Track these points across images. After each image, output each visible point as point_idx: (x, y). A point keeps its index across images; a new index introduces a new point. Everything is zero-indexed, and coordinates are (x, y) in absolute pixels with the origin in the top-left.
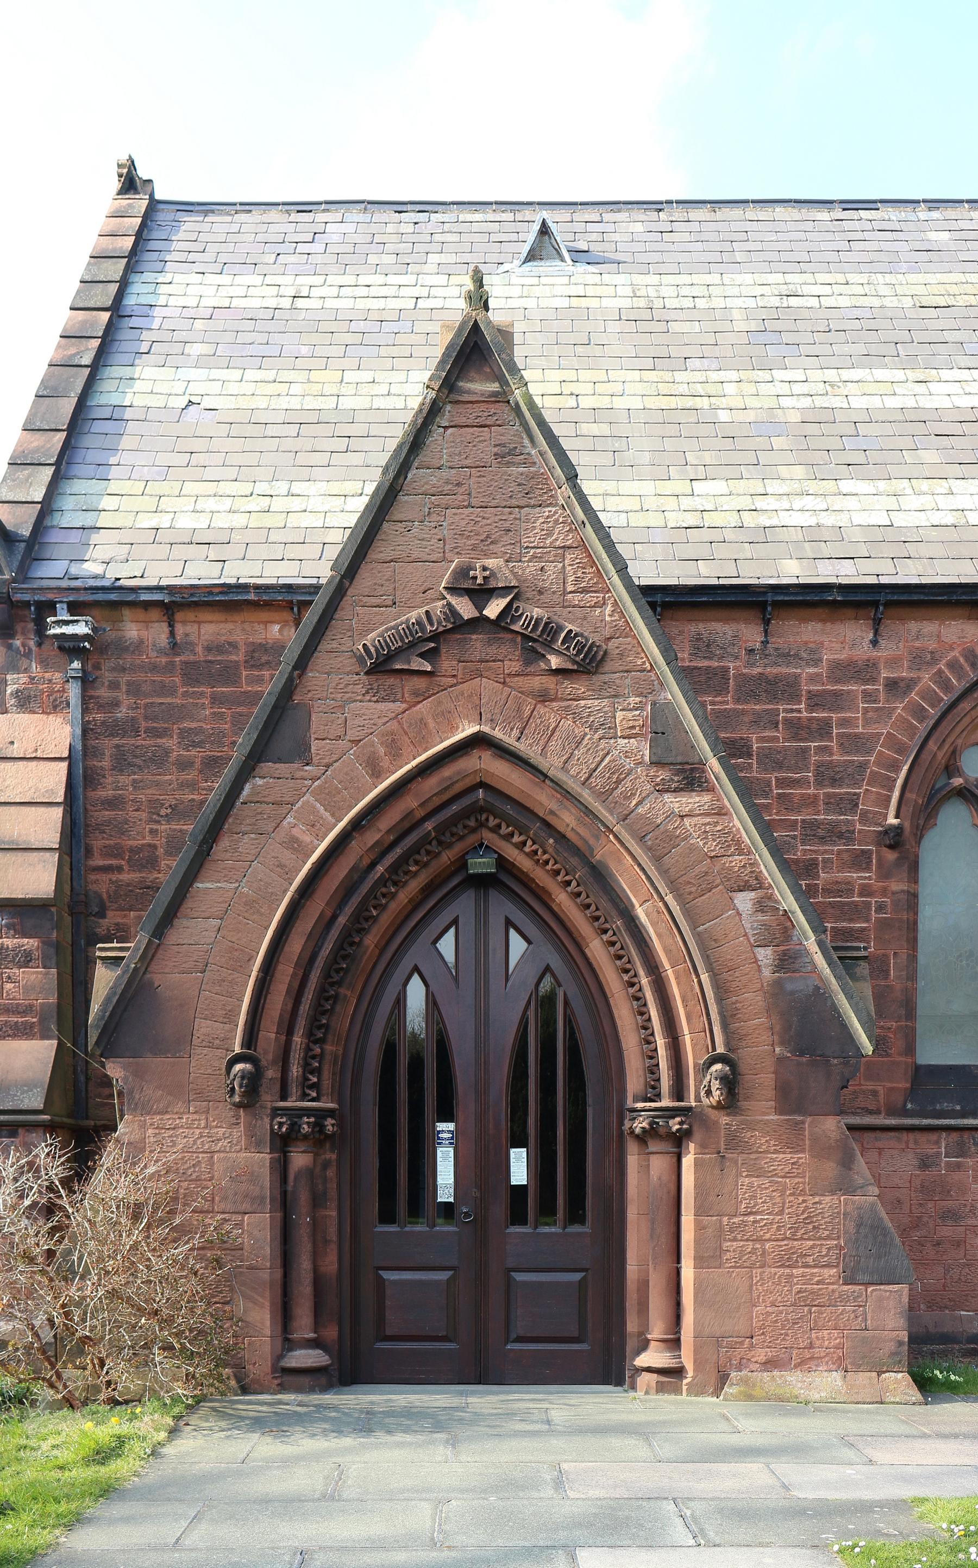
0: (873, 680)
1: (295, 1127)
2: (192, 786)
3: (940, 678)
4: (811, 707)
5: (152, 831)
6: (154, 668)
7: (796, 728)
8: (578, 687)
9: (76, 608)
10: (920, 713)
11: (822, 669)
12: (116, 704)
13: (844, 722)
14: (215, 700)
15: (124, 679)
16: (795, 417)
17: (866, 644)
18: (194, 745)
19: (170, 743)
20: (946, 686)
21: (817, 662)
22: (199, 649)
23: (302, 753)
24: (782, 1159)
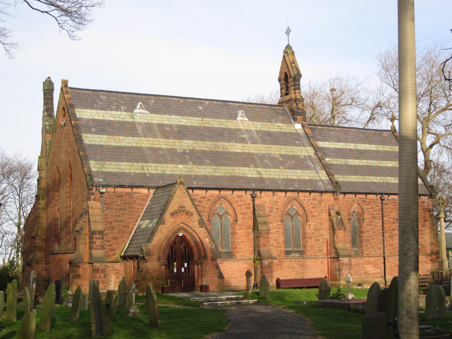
0: (206, 199)
2: (117, 212)
3: (214, 199)
4: (198, 203)
5: (112, 219)
6: (112, 195)
8: (191, 217)
10: (211, 203)
12: (106, 200)
19: (114, 206)
20: (215, 200)
21: (199, 196)
23: (164, 223)
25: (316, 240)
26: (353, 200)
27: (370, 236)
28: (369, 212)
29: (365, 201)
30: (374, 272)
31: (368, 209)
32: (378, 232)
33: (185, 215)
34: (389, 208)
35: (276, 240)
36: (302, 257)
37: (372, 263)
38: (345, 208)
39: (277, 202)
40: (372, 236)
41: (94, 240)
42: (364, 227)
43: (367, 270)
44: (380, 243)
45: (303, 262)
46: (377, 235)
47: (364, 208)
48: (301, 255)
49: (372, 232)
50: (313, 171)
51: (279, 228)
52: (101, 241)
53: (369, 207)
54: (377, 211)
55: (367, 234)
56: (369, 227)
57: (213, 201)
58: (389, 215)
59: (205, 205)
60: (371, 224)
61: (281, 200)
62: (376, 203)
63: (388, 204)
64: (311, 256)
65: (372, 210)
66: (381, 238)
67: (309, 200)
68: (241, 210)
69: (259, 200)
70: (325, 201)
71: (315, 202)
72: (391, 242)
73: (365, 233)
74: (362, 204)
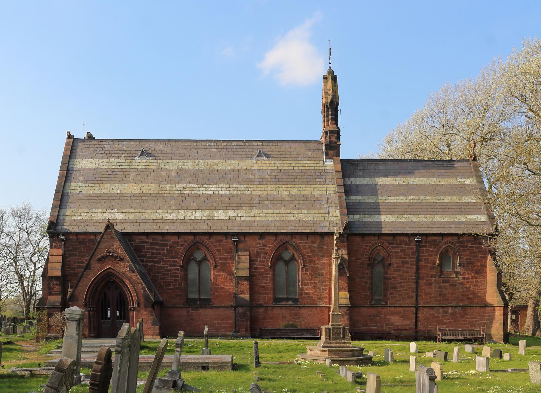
1: (90, 309)
2: (80, 259)
3: (188, 244)
6: (74, 242)
7: (168, 251)
9: (63, 235)
10: (185, 248)
11: (171, 243)
12: (69, 247)
13: (175, 250)
14: (83, 246)
15: (70, 244)
16: (176, 196)
17: (177, 239)
18: (80, 253)
19: (77, 253)
20: (189, 245)
22: (81, 240)
23: (90, 269)
24: (144, 313)
25: (315, 287)
26: (376, 243)
27: (398, 283)
28: (398, 255)
29: (393, 244)
30: (401, 324)
31: (396, 252)
32: (409, 279)
33: (114, 260)
34: (427, 251)
35: (264, 286)
36: (295, 305)
37: (399, 313)
38: (364, 252)
39: (266, 246)
40: (401, 283)
41: (51, 286)
42: (389, 273)
43: (392, 321)
44: (412, 292)
45: (296, 310)
46: (407, 282)
47: (392, 252)
48: (293, 303)
49: (401, 279)
50: (323, 211)
51: (266, 274)
52: (58, 286)
53: (399, 250)
54: (409, 255)
55: (393, 281)
56: (397, 273)
57: (186, 246)
58: (428, 259)
59: (178, 250)
60: (400, 270)
61: (270, 244)
62: (410, 245)
63: (426, 246)
64: (307, 304)
65: (403, 253)
66: (414, 286)
67: (306, 243)
68: (220, 255)
69: (244, 244)
70: (328, 244)
71: (314, 245)
72: (428, 290)
73: (390, 279)
74: (388, 247)
